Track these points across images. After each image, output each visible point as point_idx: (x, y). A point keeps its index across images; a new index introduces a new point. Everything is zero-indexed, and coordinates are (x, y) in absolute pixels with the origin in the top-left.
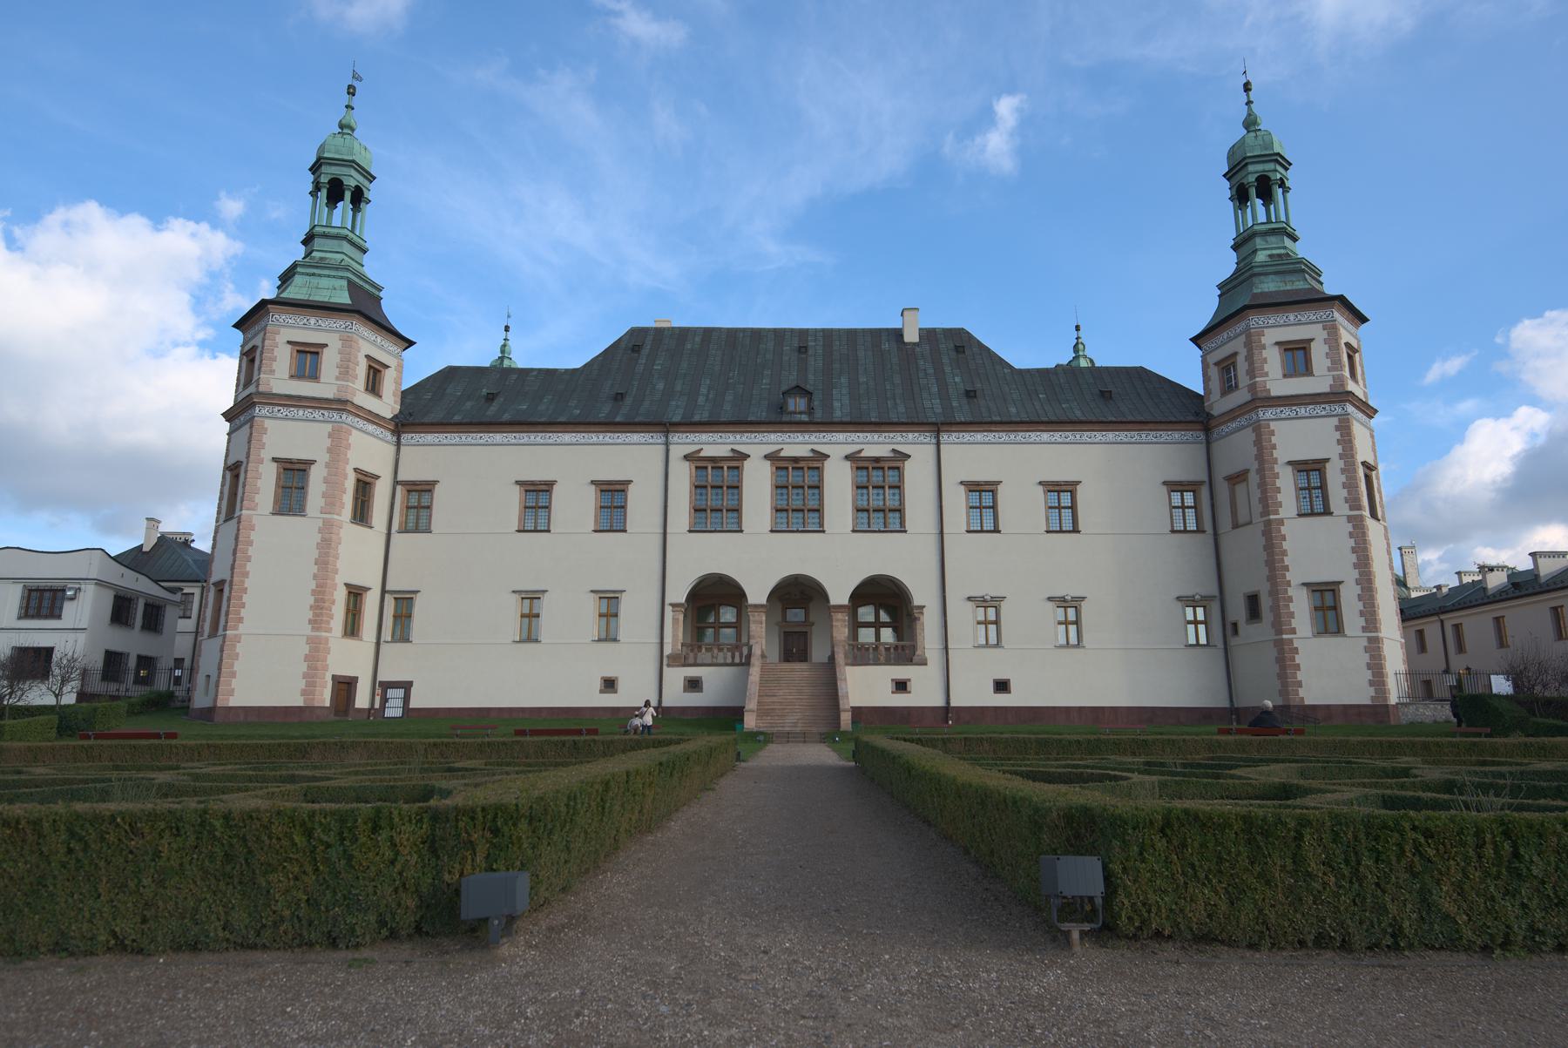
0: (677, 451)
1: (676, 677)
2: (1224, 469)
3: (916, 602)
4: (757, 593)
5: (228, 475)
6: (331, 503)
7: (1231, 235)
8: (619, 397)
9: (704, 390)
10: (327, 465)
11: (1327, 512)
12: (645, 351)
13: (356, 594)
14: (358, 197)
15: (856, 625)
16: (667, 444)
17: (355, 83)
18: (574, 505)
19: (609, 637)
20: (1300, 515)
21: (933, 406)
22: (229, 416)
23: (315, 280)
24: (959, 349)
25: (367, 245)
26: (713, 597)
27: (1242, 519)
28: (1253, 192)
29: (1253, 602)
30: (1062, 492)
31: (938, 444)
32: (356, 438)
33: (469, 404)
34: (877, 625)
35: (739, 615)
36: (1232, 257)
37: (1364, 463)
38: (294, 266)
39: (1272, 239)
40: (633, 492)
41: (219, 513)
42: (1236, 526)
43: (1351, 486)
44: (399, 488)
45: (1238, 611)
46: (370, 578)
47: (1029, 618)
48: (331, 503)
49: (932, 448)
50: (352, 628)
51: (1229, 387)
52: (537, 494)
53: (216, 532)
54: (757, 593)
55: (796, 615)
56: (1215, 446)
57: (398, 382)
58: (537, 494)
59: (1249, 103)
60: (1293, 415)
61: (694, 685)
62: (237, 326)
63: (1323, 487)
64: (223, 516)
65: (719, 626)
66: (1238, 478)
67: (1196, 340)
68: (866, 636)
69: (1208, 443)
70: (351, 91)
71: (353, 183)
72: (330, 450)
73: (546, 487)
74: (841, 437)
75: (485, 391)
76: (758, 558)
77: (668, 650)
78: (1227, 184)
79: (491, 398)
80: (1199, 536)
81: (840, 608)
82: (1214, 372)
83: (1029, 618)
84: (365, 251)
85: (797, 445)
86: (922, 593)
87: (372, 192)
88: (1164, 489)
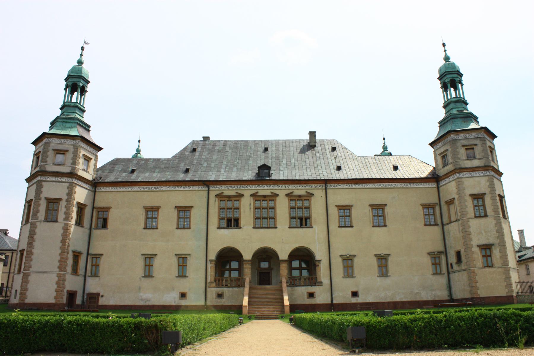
0: (212, 194)
1: (213, 292)
2: (445, 197)
3: (317, 258)
4: (247, 255)
5: (27, 204)
7: (442, 102)
8: (187, 171)
9: (224, 167)
10: (67, 201)
11: (486, 216)
12: (198, 150)
13: (77, 255)
14: (83, 91)
15: (291, 269)
16: (209, 190)
17: (85, 46)
18: (167, 218)
19: (182, 274)
20: (476, 217)
22: (28, 180)
23: (64, 124)
24: (334, 149)
25: (85, 109)
26: (227, 258)
27: (453, 219)
28: (449, 85)
29: (458, 254)
30: (379, 210)
31: (326, 189)
32: (78, 189)
33: (124, 174)
34: (300, 269)
35: (240, 265)
36: (443, 111)
37: (499, 195)
38: (57, 118)
39: (458, 104)
41: (22, 221)
42: (451, 222)
43: (494, 204)
44: (95, 210)
45: (453, 259)
46: (83, 249)
47: (365, 264)
48: (68, 217)
49: (206, 193)
50: (75, 271)
51: (445, 165)
52: (152, 212)
53: (21, 229)
54: (247, 255)
55: (265, 265)
56: (441, 189)
57: (95, 165)
58: (152, 212)
59: (445, 51)
60: (471, 176)
61: (220, 296)
62: (33, 143)
63: (484, 205)
64: (24, 223)
65: (230, 270)
66: (450, 202)
67: (432, 144)
68: (296, 273)
69: (438, 188)
70: (83, 49)
71: (81, 85)
72: (68, 194)
73: (156, 209)
74: (283, 186)
75: (130, 169)
76: (247, 240)
77: (209, 280)
78: (439, 82)
79: (133, 171)
80: (436, 227)
82: (439, 158)
83: (365, 264)
84: (84, 111)
85: (264, 190)
86: (320, 254)
87: (89, 88)
88: (421, 207)
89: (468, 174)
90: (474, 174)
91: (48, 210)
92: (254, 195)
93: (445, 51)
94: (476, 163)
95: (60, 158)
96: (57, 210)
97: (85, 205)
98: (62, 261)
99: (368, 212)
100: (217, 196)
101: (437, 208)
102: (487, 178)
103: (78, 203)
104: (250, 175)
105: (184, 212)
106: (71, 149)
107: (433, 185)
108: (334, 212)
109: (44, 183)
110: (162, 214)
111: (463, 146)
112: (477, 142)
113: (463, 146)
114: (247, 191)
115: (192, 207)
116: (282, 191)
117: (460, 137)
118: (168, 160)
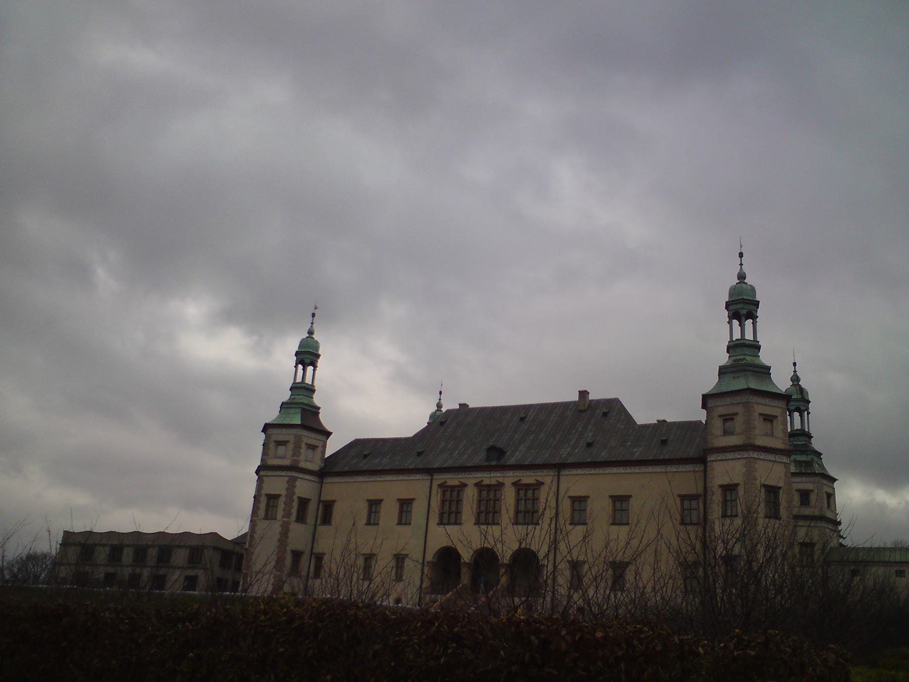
0: (436, 484)
6: (287, 514)
18: (389, 512)
21: (564, 454)
26: (448, 558)
30: (620, 501)
32: (298, 483)
40: (415, 505)
52: (374, 505)
57: (324, 452)
58: (374, 505)
59: (741, 265)
74: (510, 473)
76: (467, 537)
81: (503, 565)
89: (721, 456)
90: (730, 456)
91: (268, 506)
92: (478, 485)
93: (741, 265)
94: (732, 441)
95: (281, 450)
96: (276, 507)
97: (309, 500)
98: (280, 561)
99: (607, 504)
100: (440, 486)
101: (701, 500)
102: (744, 461)
103: (299, 498)
104: (479, 458)
105: (405, 504)
106: (291, 439)
107: (699, 468)
108: (566, 505)
109: (265, 479)
110: (384, 507)
111: (720, 416)
112: (739, 409)
113: (720, 416)
114: (471, 479)
115: (413, 500)
116: (508, 478)
117: (719, 404)
118: (407, 439)
